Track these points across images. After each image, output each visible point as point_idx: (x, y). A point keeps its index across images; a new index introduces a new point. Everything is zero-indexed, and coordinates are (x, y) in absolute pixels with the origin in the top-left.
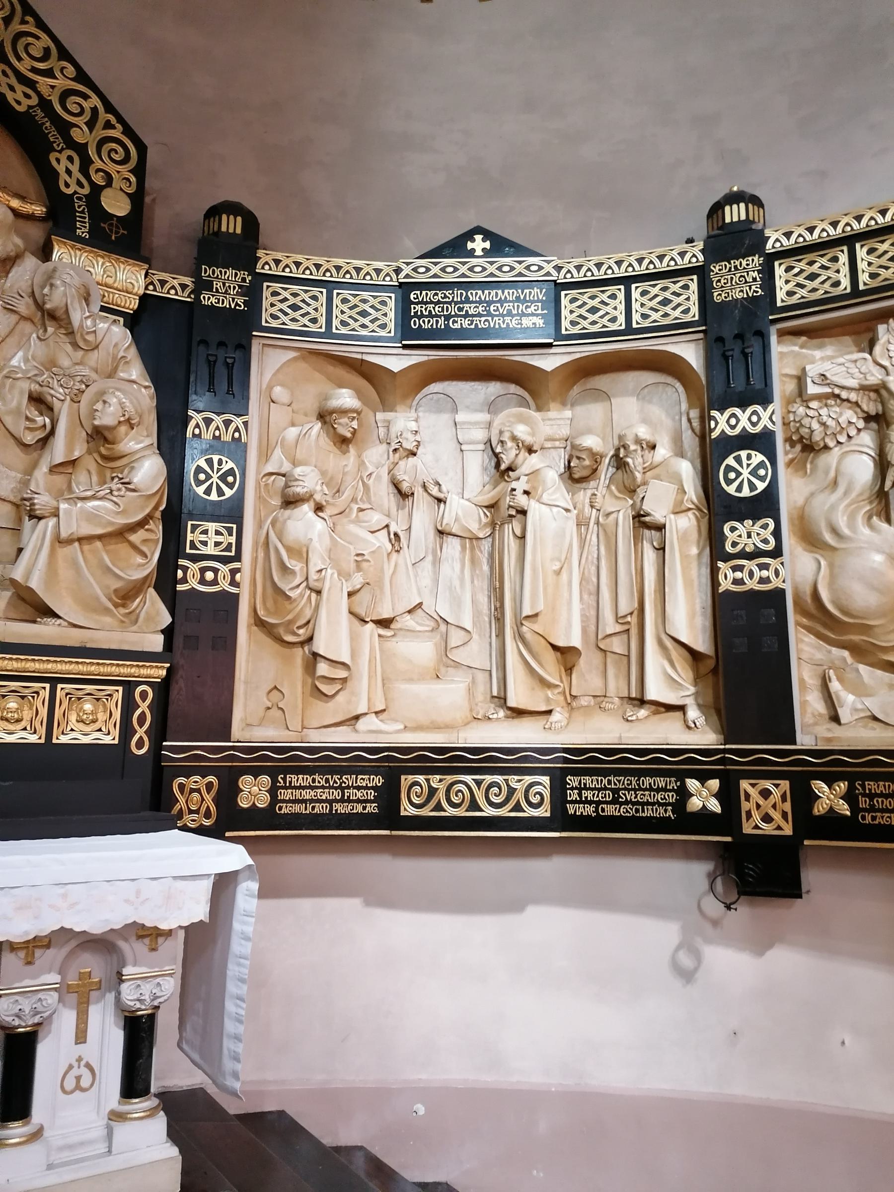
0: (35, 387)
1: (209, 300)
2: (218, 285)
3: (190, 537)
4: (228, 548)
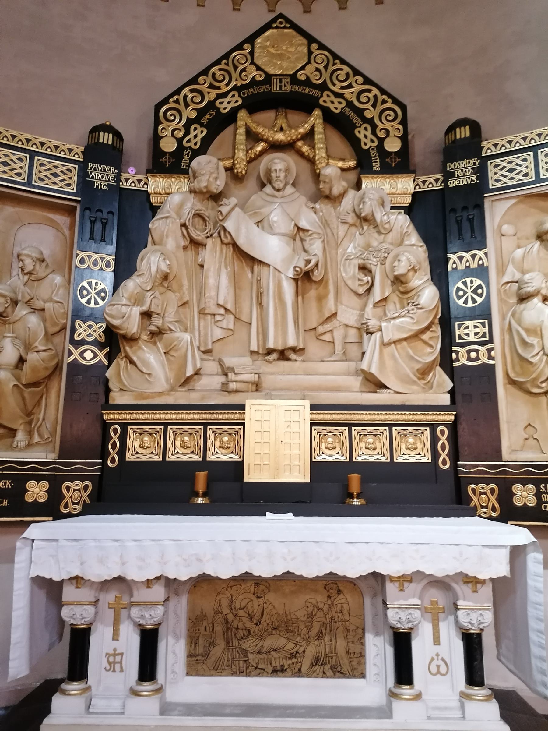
0: (361, 261)
1: (453, 183)
2: (458, 172)
3: (457, 332)
4: (484, 335)
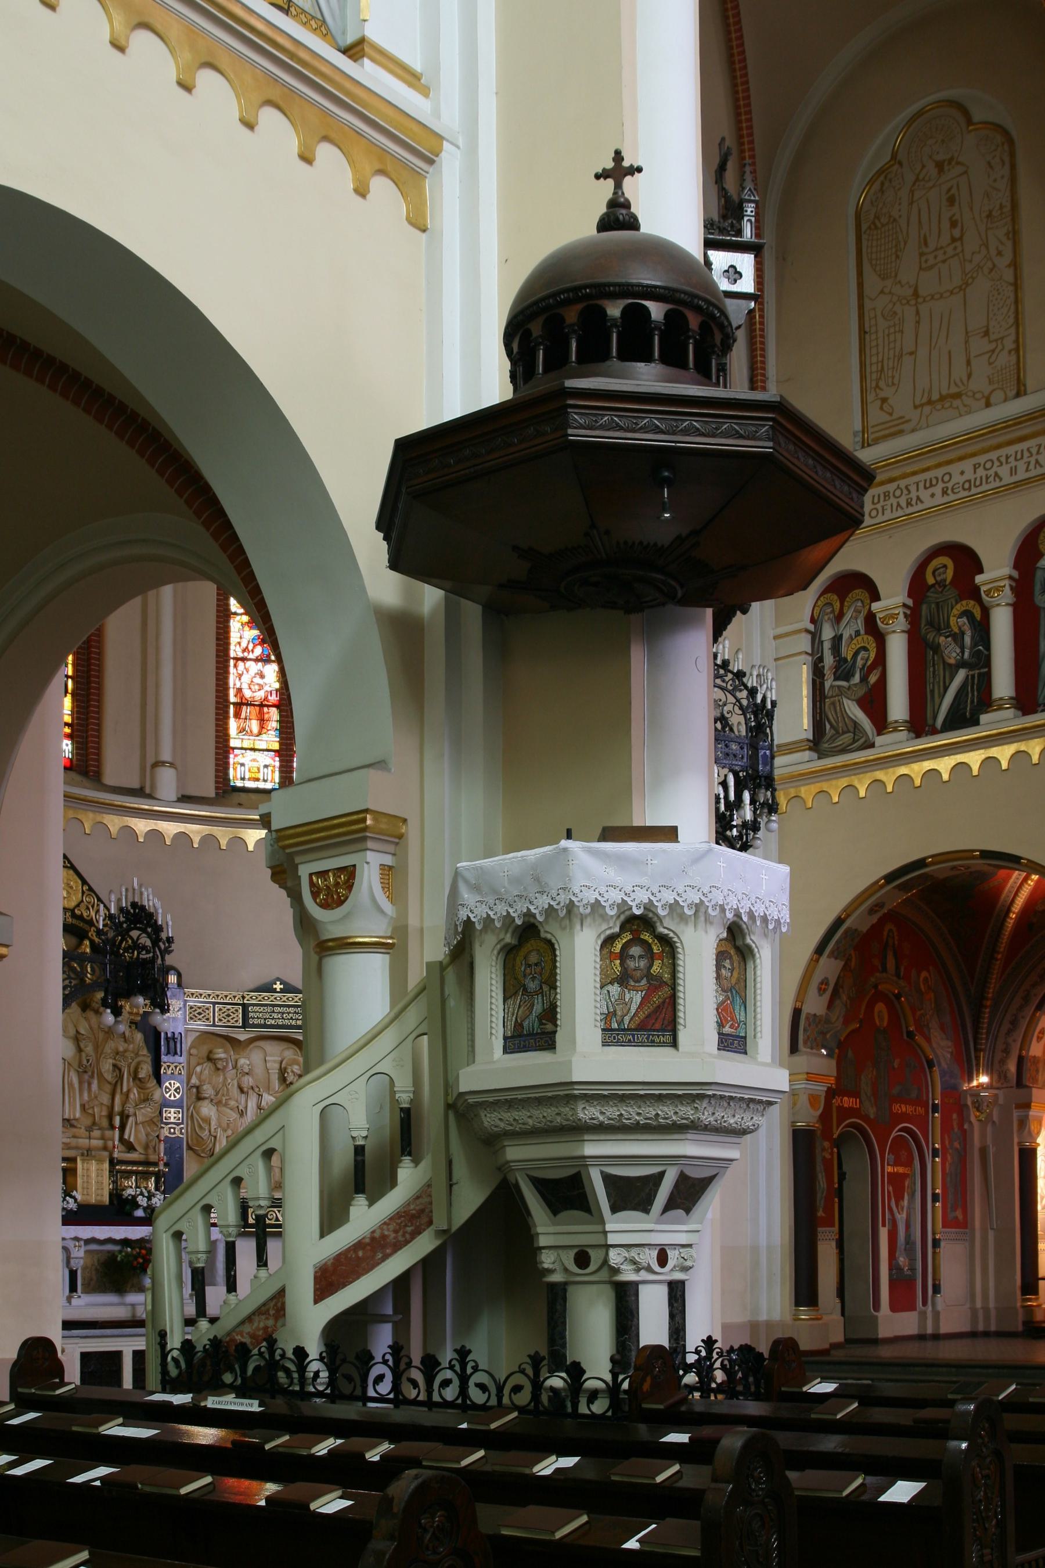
4: (179, 1119)
